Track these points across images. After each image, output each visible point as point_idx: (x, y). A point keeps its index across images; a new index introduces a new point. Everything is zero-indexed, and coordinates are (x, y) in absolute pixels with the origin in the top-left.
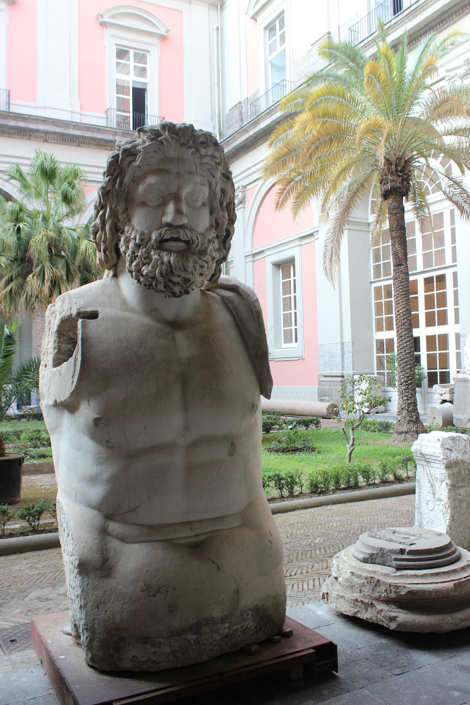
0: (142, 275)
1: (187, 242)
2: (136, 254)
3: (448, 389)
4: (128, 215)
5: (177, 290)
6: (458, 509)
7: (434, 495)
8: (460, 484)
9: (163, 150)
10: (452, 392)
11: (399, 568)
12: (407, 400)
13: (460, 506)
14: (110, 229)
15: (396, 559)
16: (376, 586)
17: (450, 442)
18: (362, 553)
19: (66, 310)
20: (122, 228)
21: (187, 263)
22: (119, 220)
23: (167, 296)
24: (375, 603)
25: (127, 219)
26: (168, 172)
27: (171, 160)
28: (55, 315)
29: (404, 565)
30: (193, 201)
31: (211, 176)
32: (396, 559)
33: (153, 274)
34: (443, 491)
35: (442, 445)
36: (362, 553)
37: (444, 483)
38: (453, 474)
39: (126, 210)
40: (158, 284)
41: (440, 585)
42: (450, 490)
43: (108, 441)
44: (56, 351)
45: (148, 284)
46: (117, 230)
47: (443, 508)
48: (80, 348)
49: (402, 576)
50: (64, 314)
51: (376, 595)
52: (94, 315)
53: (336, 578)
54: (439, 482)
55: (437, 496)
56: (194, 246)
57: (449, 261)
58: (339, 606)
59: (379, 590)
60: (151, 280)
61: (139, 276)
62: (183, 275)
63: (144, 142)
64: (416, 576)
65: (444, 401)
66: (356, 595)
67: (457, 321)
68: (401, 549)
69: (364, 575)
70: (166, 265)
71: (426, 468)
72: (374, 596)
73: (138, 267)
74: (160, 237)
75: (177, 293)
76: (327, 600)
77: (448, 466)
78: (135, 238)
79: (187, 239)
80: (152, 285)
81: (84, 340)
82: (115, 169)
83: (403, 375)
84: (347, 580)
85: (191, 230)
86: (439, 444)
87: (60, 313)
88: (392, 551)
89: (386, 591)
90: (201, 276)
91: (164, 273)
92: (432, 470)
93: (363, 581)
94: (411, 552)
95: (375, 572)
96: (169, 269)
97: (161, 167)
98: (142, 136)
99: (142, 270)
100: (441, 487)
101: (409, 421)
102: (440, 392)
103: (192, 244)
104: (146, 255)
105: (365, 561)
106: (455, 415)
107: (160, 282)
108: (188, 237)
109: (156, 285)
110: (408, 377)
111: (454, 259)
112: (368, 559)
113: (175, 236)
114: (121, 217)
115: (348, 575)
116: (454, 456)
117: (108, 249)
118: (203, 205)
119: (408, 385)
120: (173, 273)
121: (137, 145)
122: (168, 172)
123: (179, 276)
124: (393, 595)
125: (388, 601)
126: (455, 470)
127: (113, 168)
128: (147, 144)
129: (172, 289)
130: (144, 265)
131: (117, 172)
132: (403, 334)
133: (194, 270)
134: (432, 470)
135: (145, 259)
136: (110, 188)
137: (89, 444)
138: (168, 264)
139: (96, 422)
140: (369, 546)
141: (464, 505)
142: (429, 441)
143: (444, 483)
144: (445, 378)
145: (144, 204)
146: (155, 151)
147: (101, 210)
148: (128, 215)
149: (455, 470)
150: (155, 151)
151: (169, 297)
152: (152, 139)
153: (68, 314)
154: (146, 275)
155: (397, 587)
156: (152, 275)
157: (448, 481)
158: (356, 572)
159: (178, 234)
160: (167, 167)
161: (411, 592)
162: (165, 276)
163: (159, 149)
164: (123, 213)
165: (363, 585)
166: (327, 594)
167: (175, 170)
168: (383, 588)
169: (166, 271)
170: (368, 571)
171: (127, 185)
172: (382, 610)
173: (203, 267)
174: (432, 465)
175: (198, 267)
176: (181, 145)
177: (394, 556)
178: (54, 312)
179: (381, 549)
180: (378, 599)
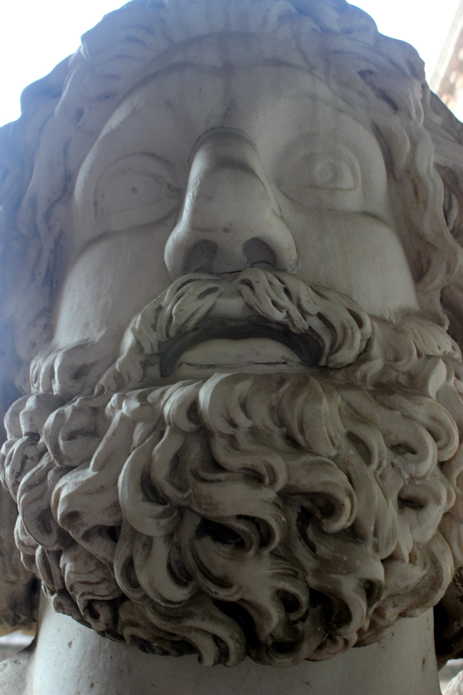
5: (258, 580)
21: (300, 400)
30: (314, 186)
31: (384, 106)
33: (105, 500)
56: (347, 355)
62: (285, 469)
70: (176, 429)
73: (37, 491)
74: (154, 327)
79: (301, 324)
90: (410, 513)
91: (161, 474)
107: (149, 543)
108: (304, 313)
113: (231, 306)
120: (218, 467)
123: (255, 477)
129: (224, 583)
133: (351, 452)
135: (71, 437)
138: (186, 425)
151: (223, 655)
159: (246, 290)
162: (169, 490)
169: (177, 461)
171: (42, 205)
173: (413, 452)
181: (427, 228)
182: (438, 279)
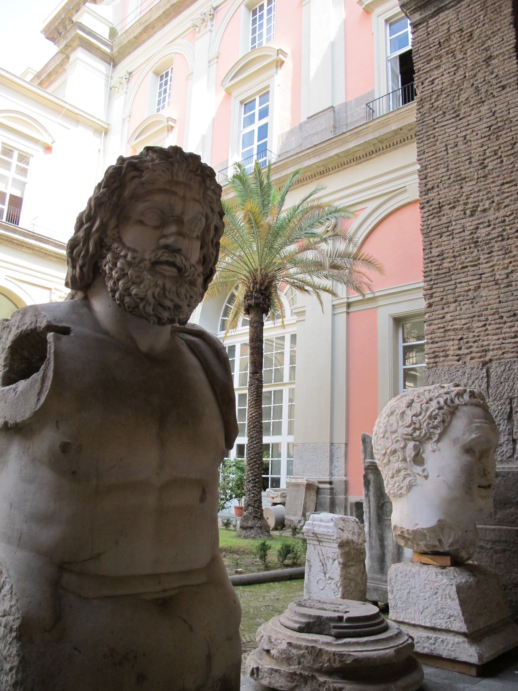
0: (130, 295)
1: (180, 270)
2: (126, 272)
3: (280, 493)
4: (118, 232)
5: (166, 315)
6: (348, 588)
7: (325, 574)
8: (350, 563)
9: (172, 171)
10: (283, 496)
11: (338, 636)
12: (253, 497)
13: (349, 585)
14: (96, 244)
15: (335, 627)
16: (317, 655)
17: (342, 522)
18: (296, 622)
19: (28, 324)
20: (109, 244)
22: (106, 236)
23: (152, 322)
24: (316, 675)
25: (116, 236)
26: (175, 194)
27: (178, 183)
28: (8, 330)
29: (344, 633)
32: (335, 627)
34: (335, 570)
35: (336, 525)
36: (296, 622)
37: (336, 562)
38: (345, 553)
39: (117, 226)
40: (147, 306)
41: (382, 652)
42: (342, 568)
43: (74, 473)
44: (7, 369)
45: (133, 306)
46: (102, 246)
47: (334, 586)
48: (52, 364)
49: (345, 644)
50: (24, 328)
51: (318, 666)
52: (65, 331)
53: (268, 651)
54: (331, 561)
55: (328, 575)
56: (186, 275)
57: (286, 379)
58: (273, 681)
59: (320, 660)
60: (138, 301)
61: (124, 296)
62: (177, 300)
63: (153, 160)
64: (358, 644)
65: (275, 504)
66: (294, 668)
67: (290, 433)
68: (339, 617)
69: (304, 644)
71: (318, 547)
72: (316, 667)
74: (155, 257)
75: (164, 319)
76: (258, 675)
77: (341, 545)
78: (125, 256)
80: (138, 307)
81: (56, 354)
82: (114, 182)
83: (252, 473)
84: (283, 652)
85: (186, 259)
86: (332, 524)
87: (18, 328)
88: (331, 619)
89: (329, 660)
91: (156, 294)
92: (324, 549)
93: (302, 652)
94: (349, 619)
95: (316, 641)
96: (162, 292)
97: (168, 187)
98: (150, 154)
99: (132, 288)
100: (333, 566)
101: (255, 517)
102: (272, 496)
103: (185, 272)
104: (137, 274)
105: (300, 630)
106: (286, 517)
107: (150, 304)
109: (144, 307)
110: (256, 475)
111: (292, 376)
112: (304, 628)
113: (171, 260)
114: (109, 233)
115: (284, 646)
116: (346, 536)
117: (87, 266)
118: (197, 237)
119: (255, 483)
120: (166, 297)
121: (146, 161)
122: (175, 194)
123: (172, 300)
124: (337, 665)
125: (330, 672)
126: (347, 549)
127: (112, 180)
128: (157, 161)
129: (160, 314)
130: (134, 283)
131: (115, 185)
132: (254, 435)
134: (324, 549)
136: (105, 199)
137: (46, 474)
139: (65, 448)
140: (304, 615)
141: (353, 584)
142: (321, 521)
143: (336, 562)
144: (276, 483)
145: (141, 222)
146: (163, 171)
147: (87, 222)
148: (118, 232)
149: (347, 549)
150: (163, 171)
151: (154, 323)
152: (162, 159)
153: (33, 326)
154: (136, 295)
155: (341, 655)
156: (142, 295)
157: (341, 560)
158: (294, 642)
160: (174, 189)
161: (357, 661)
162: (157, 298)
163: (168, 170)
164: (113, 229)
165: (303, 656)
166: (257, 669)
167: (181, 194)
168: (325, 658)
169: (159, 293)
170: (308, 641)
172: (325, 682)
174: (324, 544)
175: (188, 296)
176: (190, 171)
177: (332, 624)
178: (8, 327)
179: (319, 618)
180: (320, 671)
181: (207, 241)
182: (205, 250)
